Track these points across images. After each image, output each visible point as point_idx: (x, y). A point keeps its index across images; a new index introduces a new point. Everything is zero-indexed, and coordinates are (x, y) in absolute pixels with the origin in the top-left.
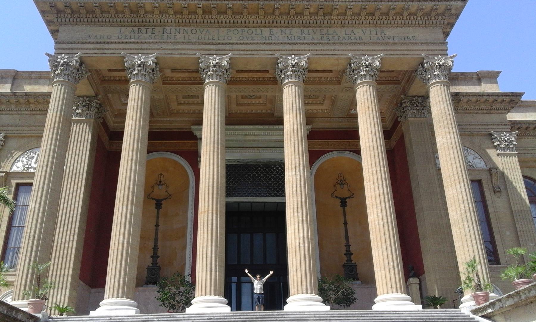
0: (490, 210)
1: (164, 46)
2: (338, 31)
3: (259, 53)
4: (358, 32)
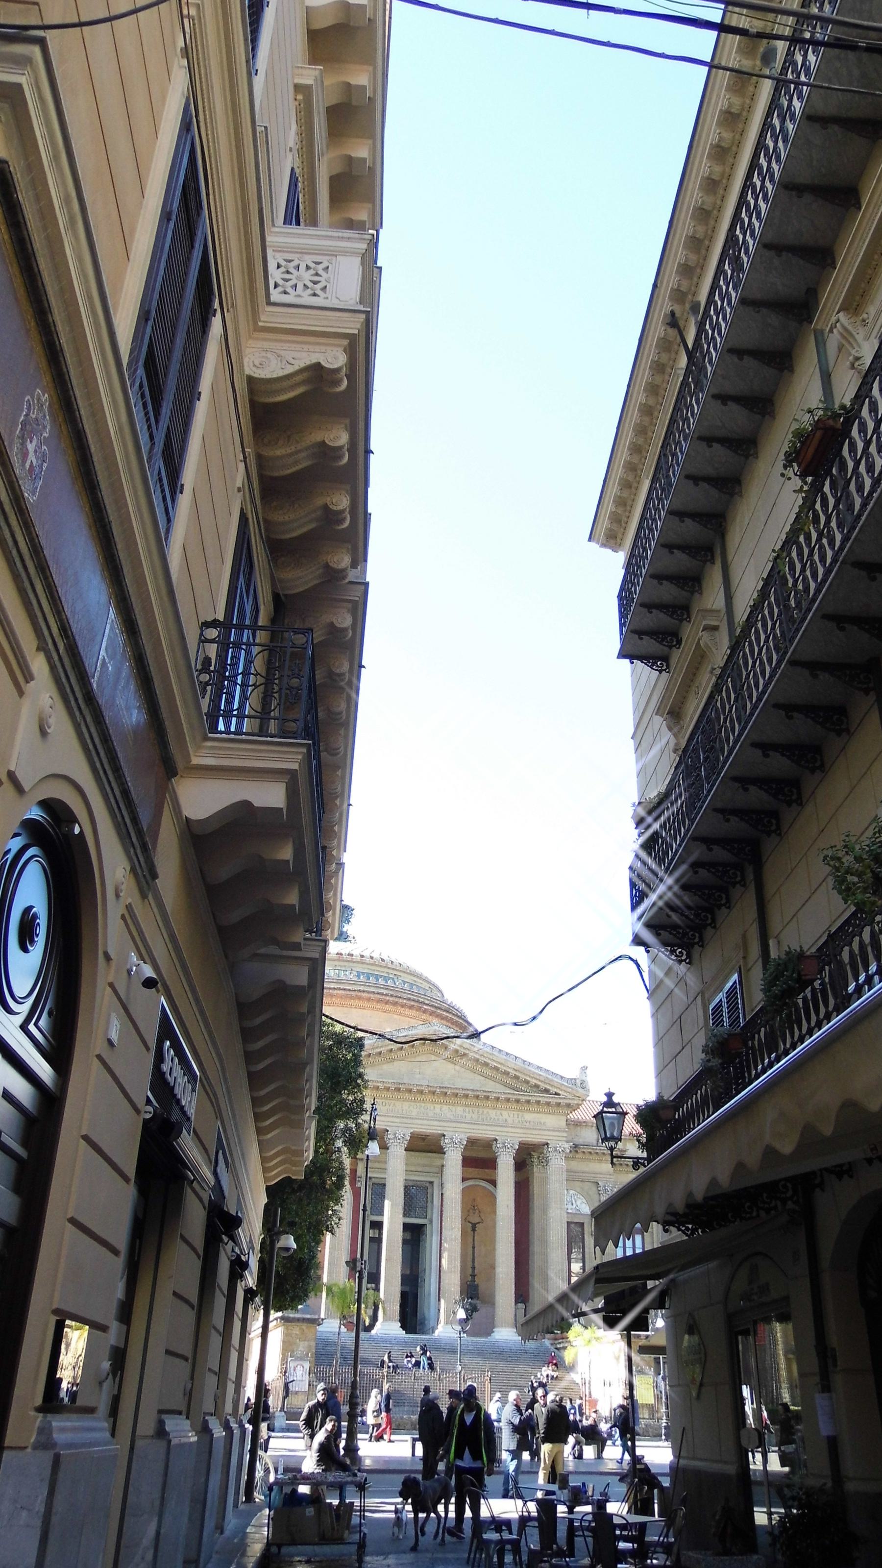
2: (490, 1111)
4: (505, 1114)
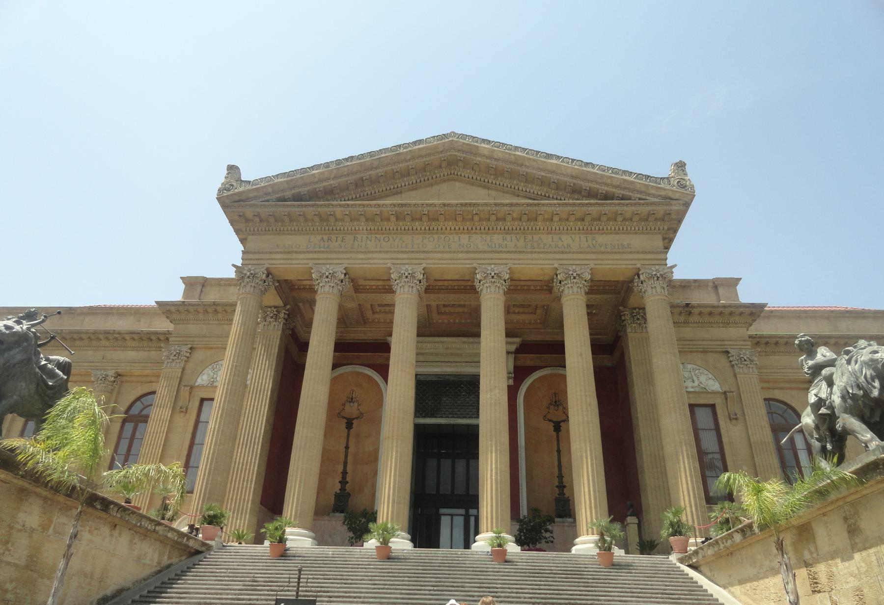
0: (725, 440)
1: (354, 256)
3: (455, 262)
4: (566, 239)
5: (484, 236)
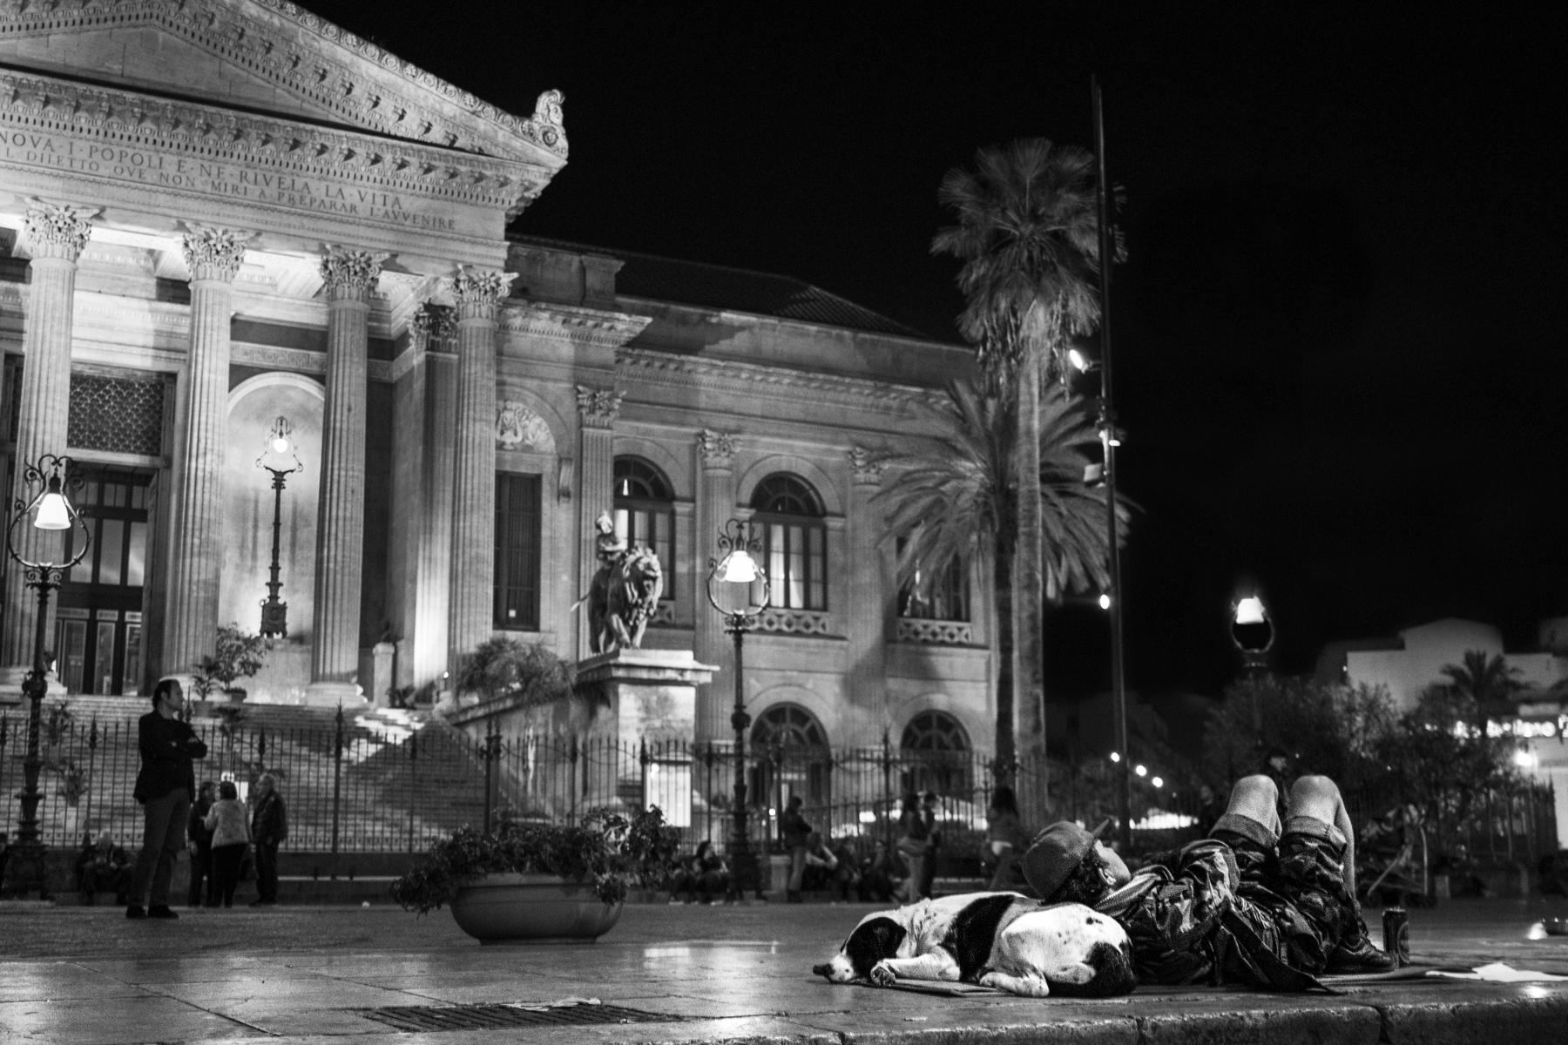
5: (206, 164)
